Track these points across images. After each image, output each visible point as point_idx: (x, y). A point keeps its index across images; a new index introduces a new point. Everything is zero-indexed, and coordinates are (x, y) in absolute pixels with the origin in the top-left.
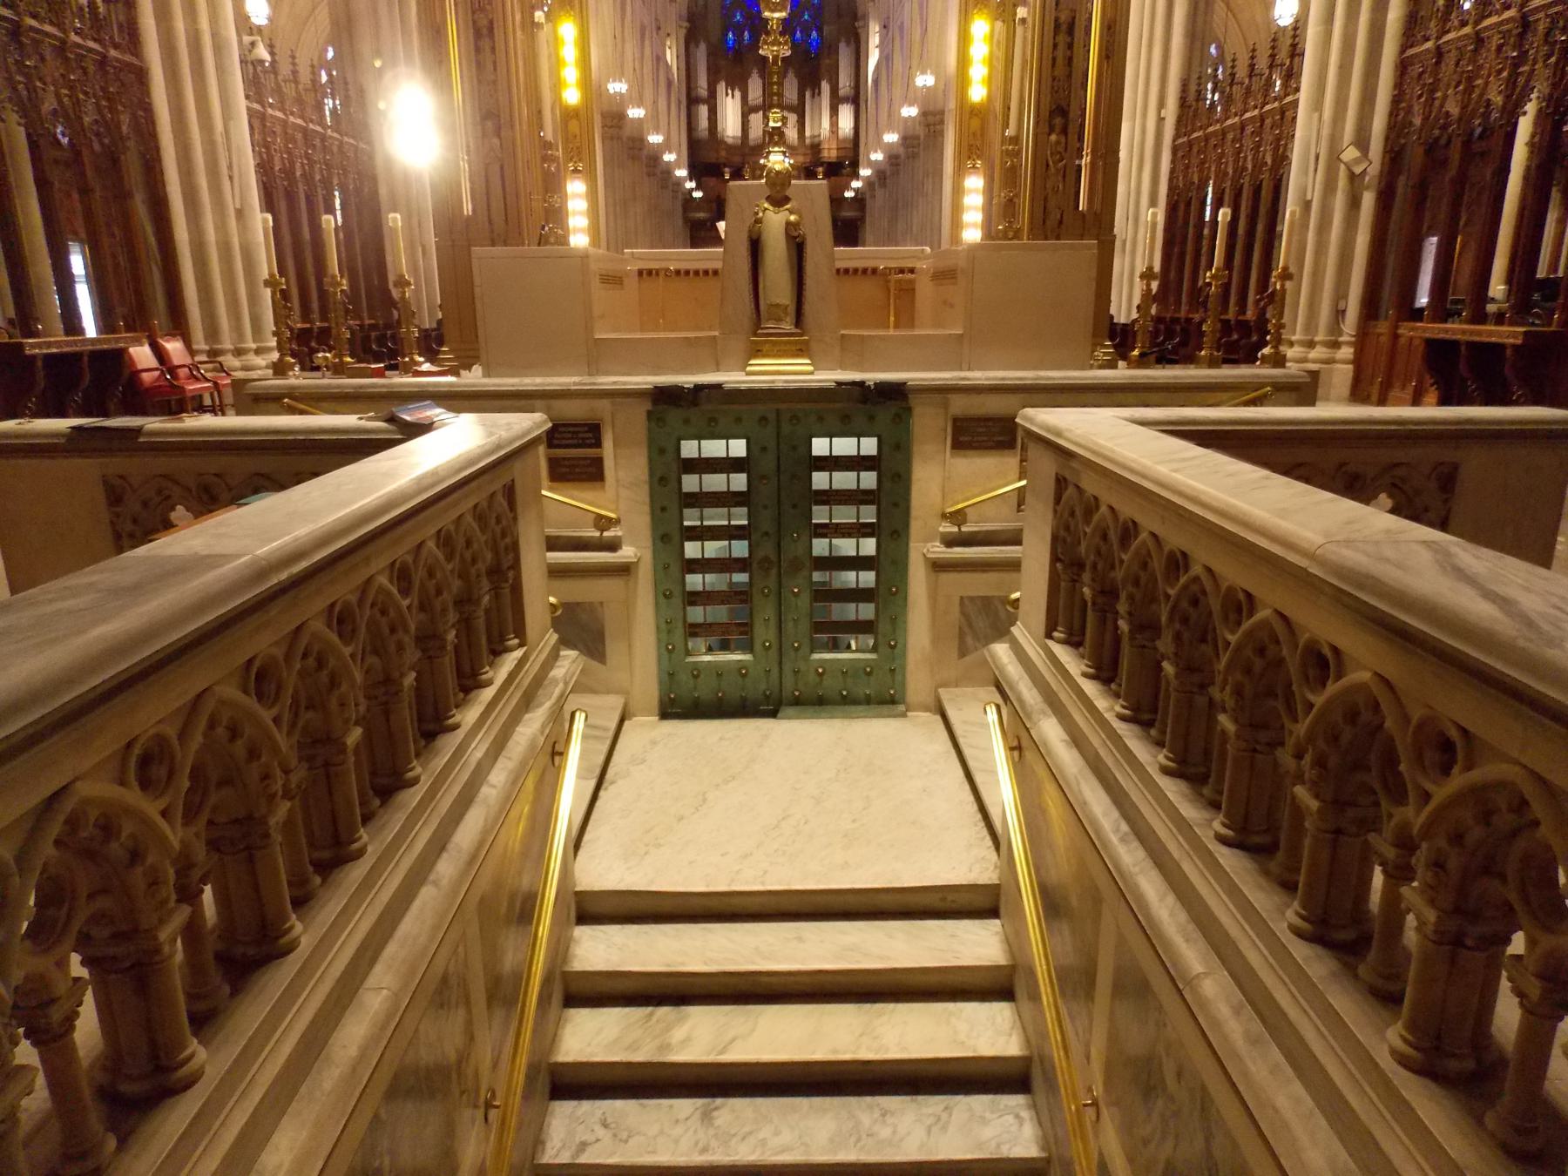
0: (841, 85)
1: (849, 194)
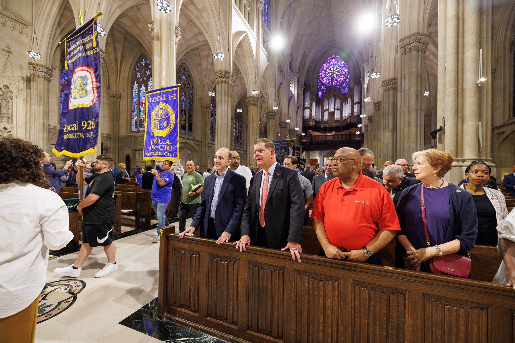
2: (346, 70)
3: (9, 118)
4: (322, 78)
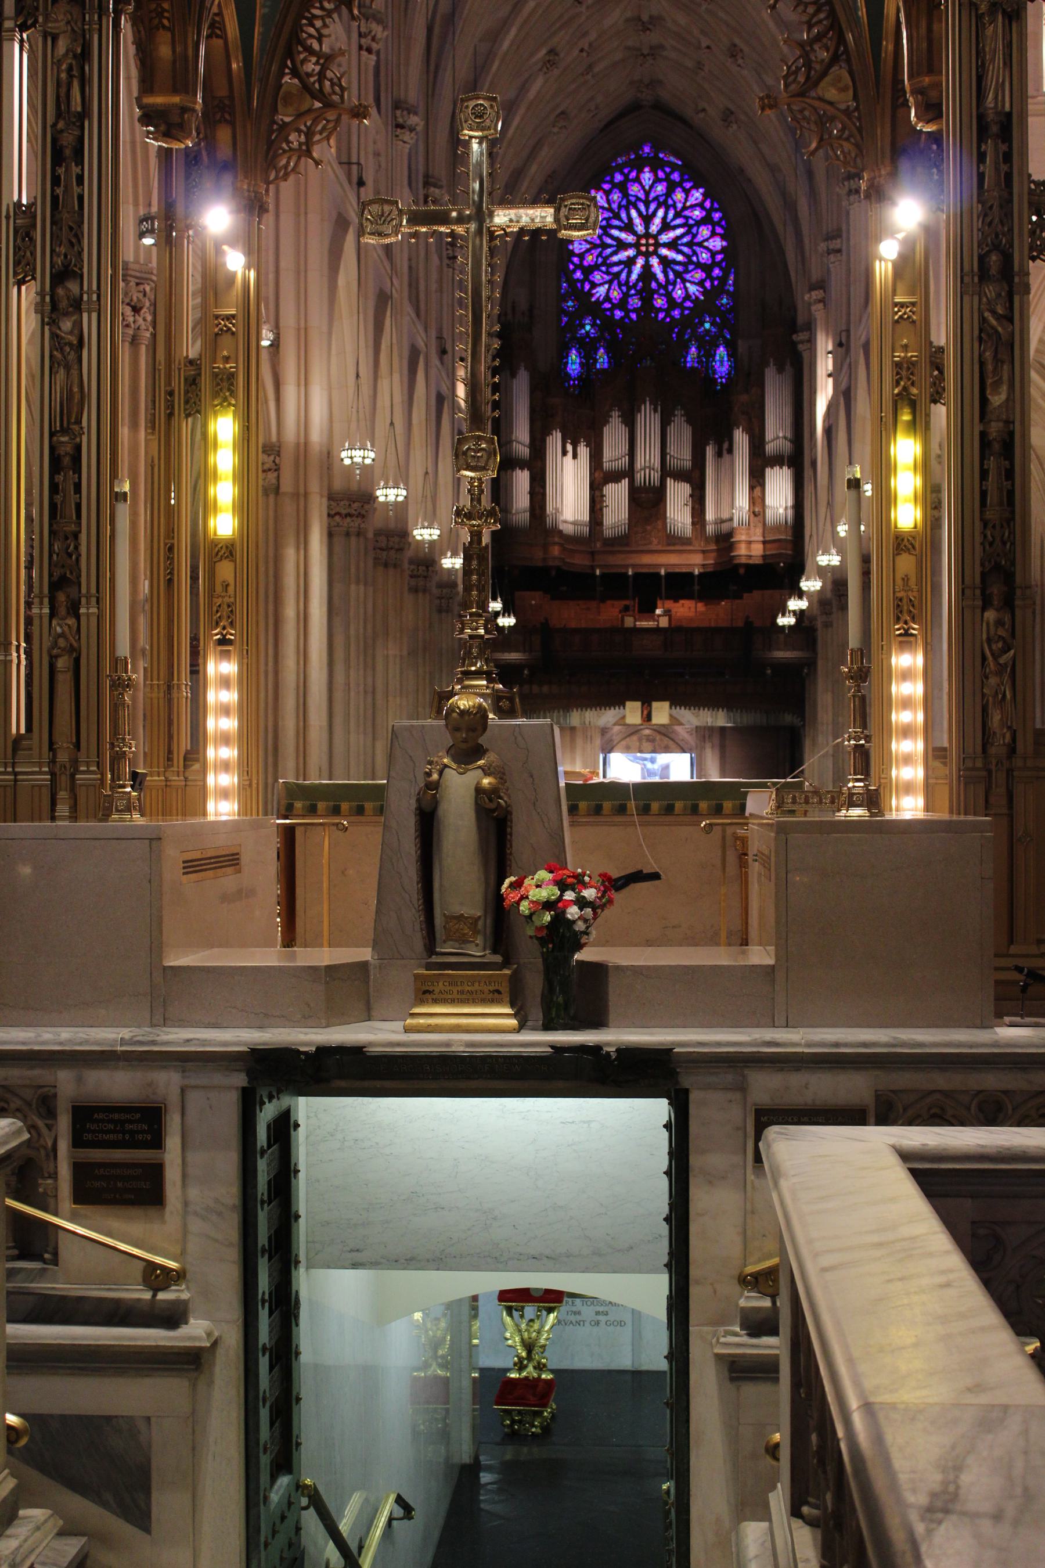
0: (769, 435)
1: (785, 621)
2: (717, 244)
4: (579, 267)
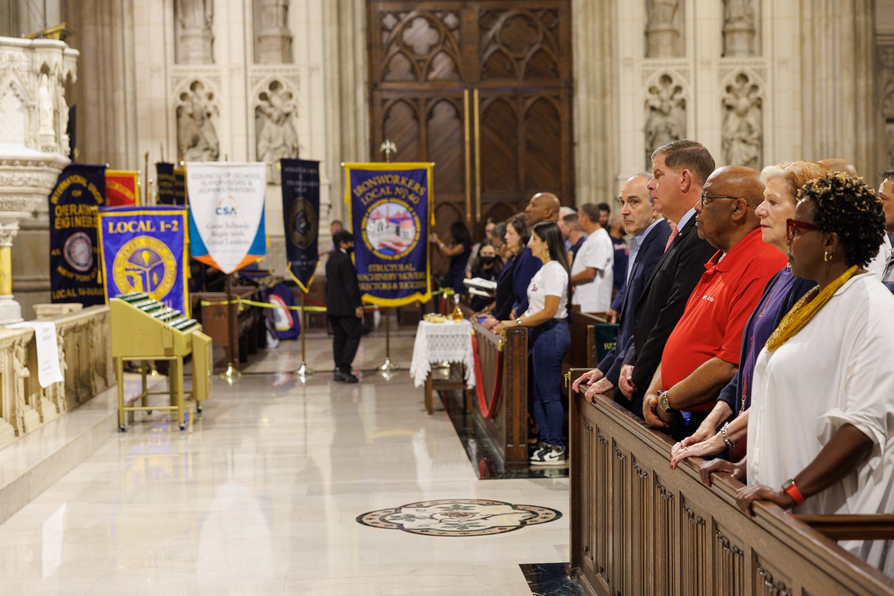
3: (751, 32)
